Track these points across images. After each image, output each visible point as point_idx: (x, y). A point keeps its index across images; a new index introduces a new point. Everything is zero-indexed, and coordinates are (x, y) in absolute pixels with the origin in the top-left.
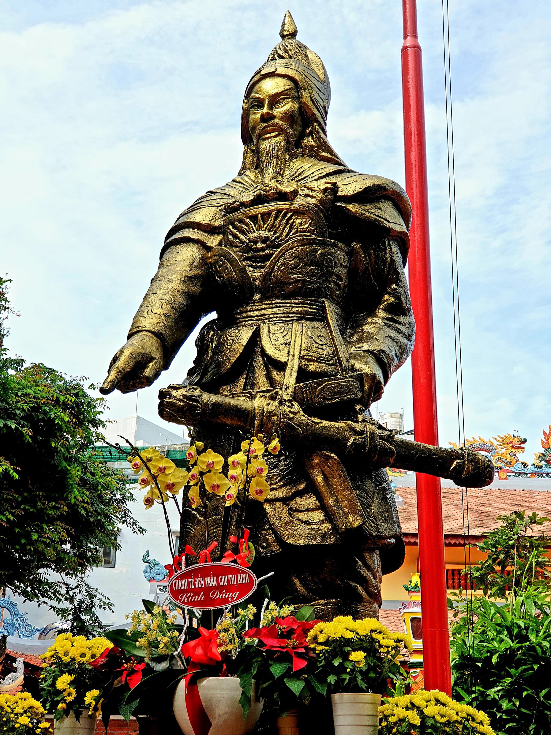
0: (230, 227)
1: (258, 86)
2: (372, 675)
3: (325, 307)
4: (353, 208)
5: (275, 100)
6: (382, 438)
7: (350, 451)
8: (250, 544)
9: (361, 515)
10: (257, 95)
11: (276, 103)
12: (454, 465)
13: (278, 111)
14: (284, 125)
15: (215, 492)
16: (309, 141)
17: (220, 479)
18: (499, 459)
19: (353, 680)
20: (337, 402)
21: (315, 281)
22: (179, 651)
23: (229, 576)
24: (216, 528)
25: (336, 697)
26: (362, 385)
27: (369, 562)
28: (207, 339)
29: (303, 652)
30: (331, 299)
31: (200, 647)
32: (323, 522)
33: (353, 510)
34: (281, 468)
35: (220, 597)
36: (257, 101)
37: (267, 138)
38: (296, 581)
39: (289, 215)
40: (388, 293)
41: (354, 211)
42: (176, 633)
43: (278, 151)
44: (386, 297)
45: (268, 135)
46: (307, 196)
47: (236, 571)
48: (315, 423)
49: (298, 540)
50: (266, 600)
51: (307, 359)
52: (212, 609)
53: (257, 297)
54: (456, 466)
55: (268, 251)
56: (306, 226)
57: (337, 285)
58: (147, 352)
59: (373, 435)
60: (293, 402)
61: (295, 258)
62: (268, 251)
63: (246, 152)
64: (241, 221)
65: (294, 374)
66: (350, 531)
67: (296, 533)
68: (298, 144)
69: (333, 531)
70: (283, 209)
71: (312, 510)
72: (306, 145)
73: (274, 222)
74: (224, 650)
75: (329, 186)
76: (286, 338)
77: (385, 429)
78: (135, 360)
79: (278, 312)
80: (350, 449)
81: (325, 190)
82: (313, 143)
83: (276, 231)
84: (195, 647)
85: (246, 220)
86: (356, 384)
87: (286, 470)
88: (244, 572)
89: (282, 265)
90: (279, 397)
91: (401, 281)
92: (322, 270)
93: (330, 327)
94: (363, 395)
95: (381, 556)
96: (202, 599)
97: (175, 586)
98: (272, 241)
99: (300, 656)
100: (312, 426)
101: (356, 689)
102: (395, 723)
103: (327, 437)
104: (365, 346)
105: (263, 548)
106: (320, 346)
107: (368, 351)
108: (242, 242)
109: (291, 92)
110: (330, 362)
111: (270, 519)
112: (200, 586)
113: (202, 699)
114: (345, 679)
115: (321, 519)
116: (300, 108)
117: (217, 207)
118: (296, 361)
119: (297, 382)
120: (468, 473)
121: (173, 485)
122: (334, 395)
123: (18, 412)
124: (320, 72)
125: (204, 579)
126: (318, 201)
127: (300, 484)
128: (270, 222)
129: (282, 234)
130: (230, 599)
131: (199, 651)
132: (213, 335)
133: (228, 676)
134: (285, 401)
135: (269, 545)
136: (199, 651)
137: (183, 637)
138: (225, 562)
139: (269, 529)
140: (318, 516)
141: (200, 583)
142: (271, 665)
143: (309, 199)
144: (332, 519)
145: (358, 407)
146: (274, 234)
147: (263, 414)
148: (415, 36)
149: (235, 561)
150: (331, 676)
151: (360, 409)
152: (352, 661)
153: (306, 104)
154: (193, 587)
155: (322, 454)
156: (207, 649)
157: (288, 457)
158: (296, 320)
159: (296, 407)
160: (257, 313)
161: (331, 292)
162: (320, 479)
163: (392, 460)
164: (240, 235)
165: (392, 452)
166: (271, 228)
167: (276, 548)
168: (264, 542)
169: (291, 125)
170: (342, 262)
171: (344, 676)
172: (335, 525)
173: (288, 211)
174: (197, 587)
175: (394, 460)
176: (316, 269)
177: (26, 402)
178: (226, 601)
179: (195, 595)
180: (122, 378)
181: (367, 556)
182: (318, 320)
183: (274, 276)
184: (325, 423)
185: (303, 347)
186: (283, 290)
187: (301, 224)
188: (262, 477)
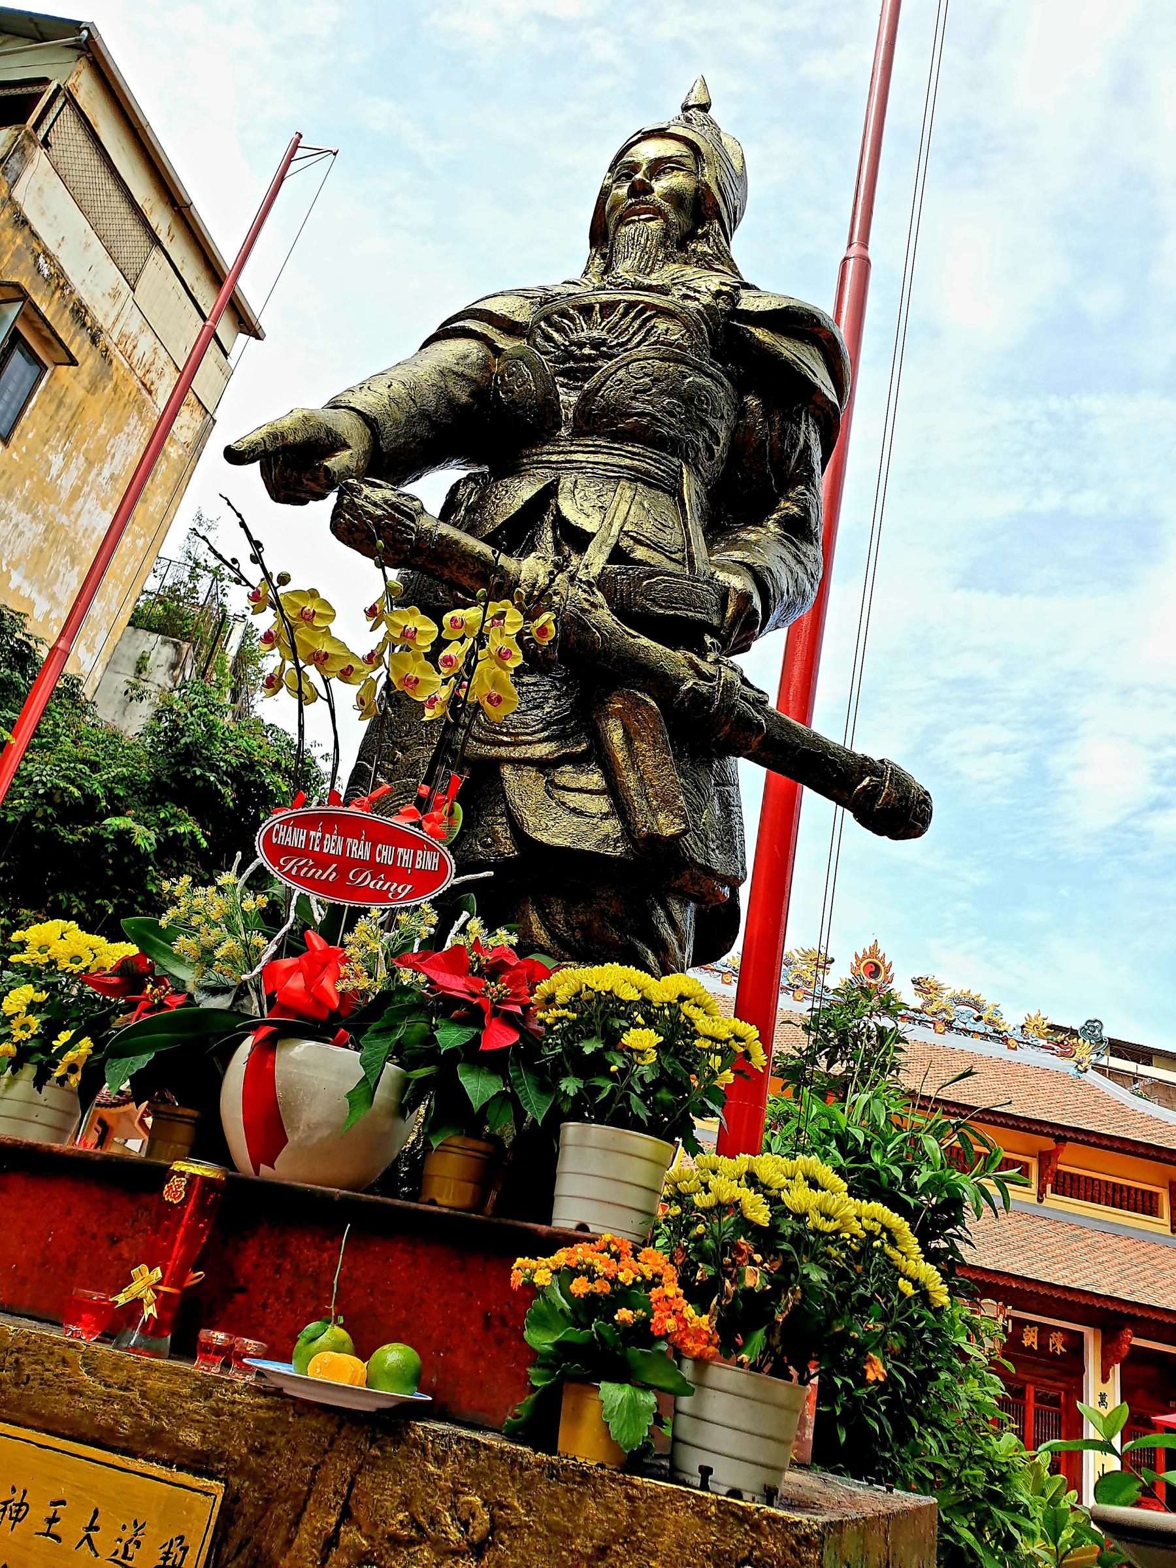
0: (542, 324)
1: (632, 150)
2: (665, 1095)
3: (682, 473)
4: (760, 334)
5: (658, 167)
6: (744, 698)
7: (682, 701)
8: (457, 806)
9: (684, 817)
10: (630, 159)
11: (659, 174)
12: (865, 783)
13: (660, 186)
14: (666, 206)
15: (409, 692)
16: (702, 247)
17: (423, 669)
18: (798, 976)
19: (619, 1095)
20: (675, 616)
21: (671, 424)
22: (255, 973)
23: (400, 850)
24: (405, 798)
25: (571, 1130)
26: (724, 608)
27: (678, 917)
28: (461, 491)
29: (517, 1014)
30: (695, 467)
31: (301, 975)
32: (606, 816)
33: (667, 803)
34: (548, 710)
35: (371, 886)
36: (627, 168)
37: (633, 222)
38: (534, 917)
39: (648, 313)
40: (788, 499)
41: (761, 337)
42: (259, 940)
43: (647, 239)
44: (783, 504)
45: (636, 218)
46: (685, 297)
47: (415, 844)
48: (629, 634)
49: (554, 836)
50: (465, 915)
51: (632, 538)
52: (347, 904)
53: (564, 432)
54: (868, 786)
55: (600, 363)
56: (674, 338)
57: (709, 449)
58: (339, 431)
59: (729, 686)
60: (595, 589)
61: (647, 375)
62: (600, 363)
63: (591, 258)
64: (564, 314)
65: (607, 551)
66: (654, 839)
67: (552, 823)
68: (682, 245)
69: (623, 835)
70: (642, 302)
71: (591, 792)
72: (694, 251)
73: (621, 319)
74: (350, 988)
75: (725, 289)
76: (603, 499)
77: (751, 686)
78: (311, 431)
79: (596, 460)
80: (683, 699)
81: (718, 294)
82: (706, 249)
83: (620, 334)
84: (289, 972)
85: (571, 312)
86: (713, 598)
87: (556, 714)
88: (431, 848)
89: (621, 381)
90: (571, 568)
91: (814, 485)
92: (688, 411)
93: (683, 505)
94: (722, 623)
95: (699, 916)
96: (331, 879)
97: (277, 836)
98: (611, 348)
99: (510, 1020)
100: (622, 637)
101: (624, 1120)
102: (707, 1211)
103: (646, 666)
104: (737, 555)
105: (485, 845)
106: (660, 526)
107: (741, 563)
108: (557, 347)
109: (686, 161)
110: (673, 556)
111: (509, 794)
112: (332, 852)
113: (278, 1082)
114: (600, 1089)
115: (606, 809)
116: (697, 190)
117: (528, 298)
118: (615, 530)
119: (609, 561)
120: (887, 804)
121: (326, 655)
122: (670, 602)
123: (222, 764)
124: (737, 163)
125: (345, 841)
126: (704, 306)
127: (579, 744)
128: (614, 318)
129: (629, 340)
130: (390, 895)
131: (296, 983)
132: (473, 489)
133: (347, 1048)
134: (580, 581)
135: (496, 841)
136: (296, 983)
137: (272, 948)
138: (401, 822)
139: (502, 815)
140: (601, 804)
141: (333, 845)
142: (436, 1027)
143: (688, 303)
144: (625, 813)
145: (708, 639)
146: (616, 338)
147: (534, 585)
148: (865, 242)
149: (419, 825)
150: (571, 1078)
151: (712, 643)
152: (630, 1050)
153: (706, 185)
154: (317, 849)
155: (629, 693)
156: (312, 978)
157: (565, 694)
158: (627, 479)
159: (600, 598)
160: (561, 458)
161: (697, 455)
162: (616, 736)
163: (755, 741)
164: (556, 335)
165: (760, 725)
166: (613, 328)
167: (508, 849)
168: (487, 836)
169: (677, 212)
170: (725, 412)
171: (599, 1082)
172: (630, 824)
173: (648, 306)
174: (325, 851)
175: (760, 743)
176: (679, 406)
177: (236, 755)
178: (380, 896)
179: (317, 865)
180: (277, 451)
181: (675, 907)
182: (664, 491)
183: (602, 396)
184: (644, 641)
185: (630, 519)
186: (615, 425)
187: (667, 331)
188: (505, 668)
